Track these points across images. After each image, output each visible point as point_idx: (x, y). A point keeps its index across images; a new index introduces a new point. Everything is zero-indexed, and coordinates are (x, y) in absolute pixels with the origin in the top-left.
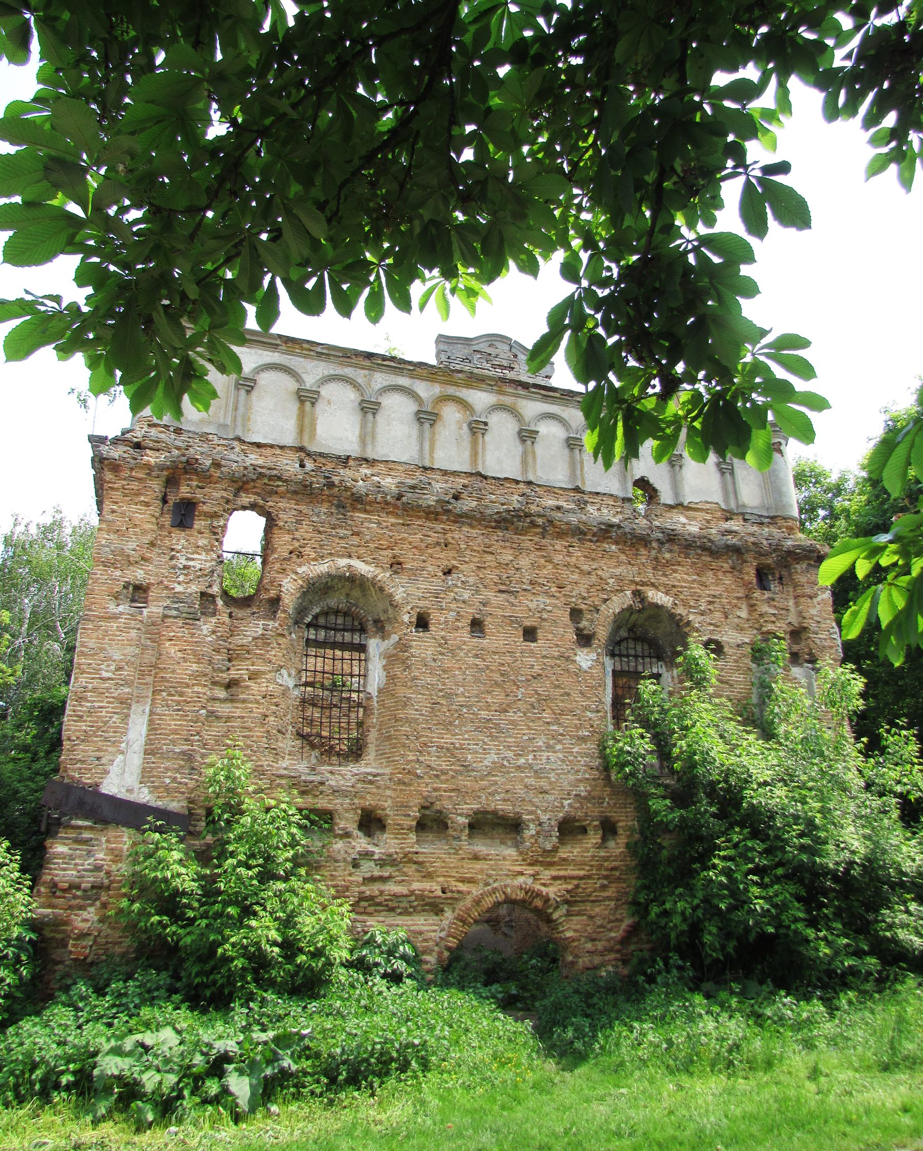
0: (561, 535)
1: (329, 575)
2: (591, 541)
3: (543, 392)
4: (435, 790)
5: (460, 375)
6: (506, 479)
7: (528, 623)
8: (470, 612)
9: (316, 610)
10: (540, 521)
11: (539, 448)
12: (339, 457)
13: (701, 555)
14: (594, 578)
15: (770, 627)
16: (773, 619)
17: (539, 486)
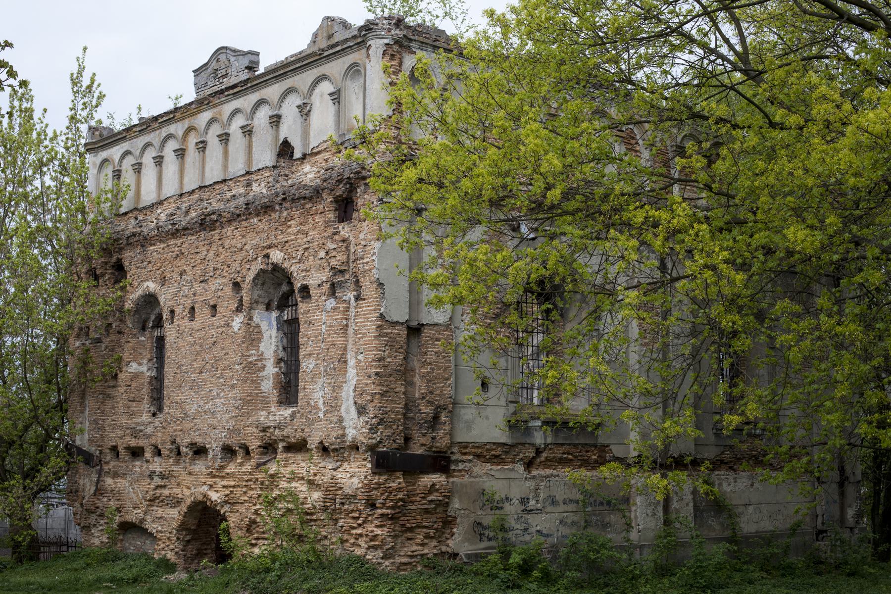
0: (230, 222)
1: (143, 297)
2: (243, 220)
3: (231, 92)
4: (175, 431)
5: (193, 106)
6: (215, 183)
7: (211, 303)
8: (188, 303)
9: (153, 317)
10: (214, 217)
11: (231, 144)
12: (150, 206)
13: (305, 204)
14: (244, 253)
15: (333, 262)
16: (334, 253)
17: (231, 180)
